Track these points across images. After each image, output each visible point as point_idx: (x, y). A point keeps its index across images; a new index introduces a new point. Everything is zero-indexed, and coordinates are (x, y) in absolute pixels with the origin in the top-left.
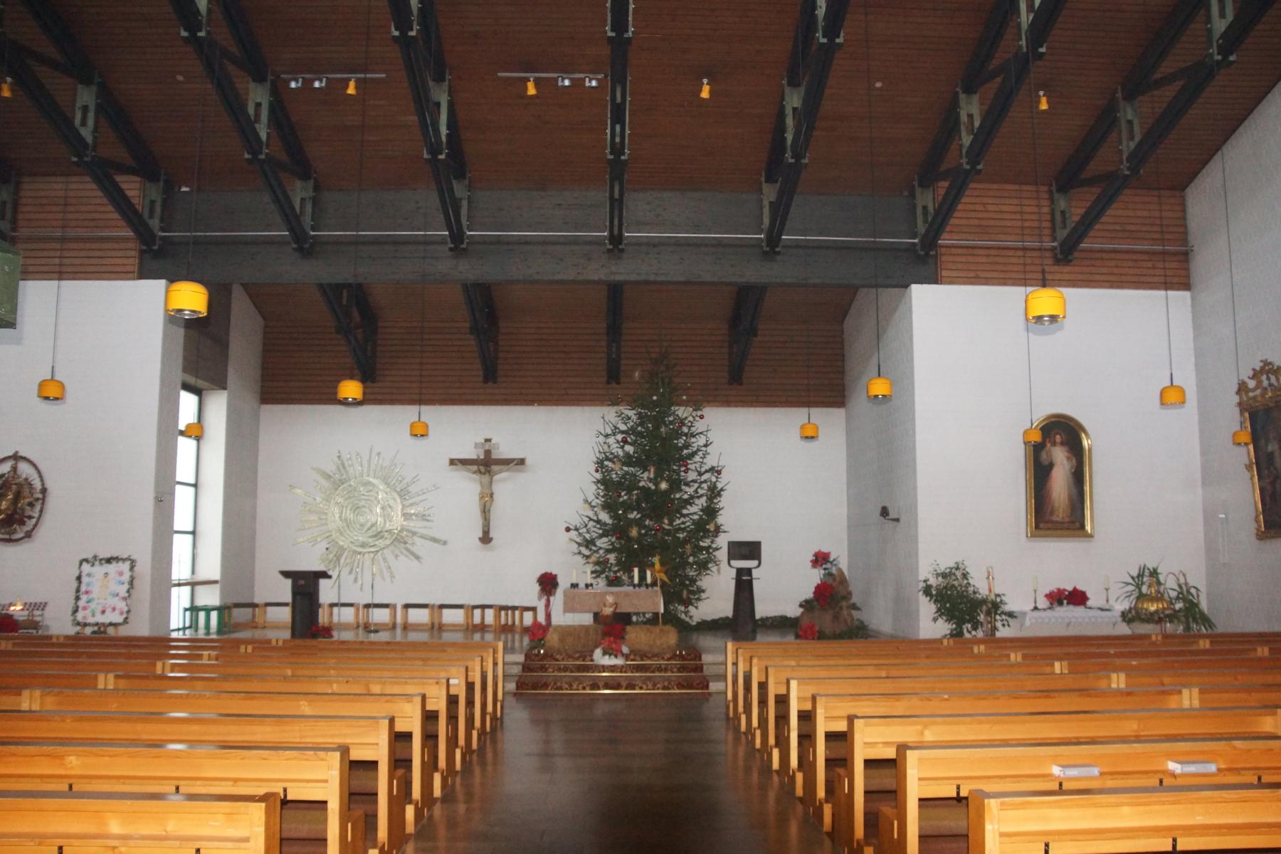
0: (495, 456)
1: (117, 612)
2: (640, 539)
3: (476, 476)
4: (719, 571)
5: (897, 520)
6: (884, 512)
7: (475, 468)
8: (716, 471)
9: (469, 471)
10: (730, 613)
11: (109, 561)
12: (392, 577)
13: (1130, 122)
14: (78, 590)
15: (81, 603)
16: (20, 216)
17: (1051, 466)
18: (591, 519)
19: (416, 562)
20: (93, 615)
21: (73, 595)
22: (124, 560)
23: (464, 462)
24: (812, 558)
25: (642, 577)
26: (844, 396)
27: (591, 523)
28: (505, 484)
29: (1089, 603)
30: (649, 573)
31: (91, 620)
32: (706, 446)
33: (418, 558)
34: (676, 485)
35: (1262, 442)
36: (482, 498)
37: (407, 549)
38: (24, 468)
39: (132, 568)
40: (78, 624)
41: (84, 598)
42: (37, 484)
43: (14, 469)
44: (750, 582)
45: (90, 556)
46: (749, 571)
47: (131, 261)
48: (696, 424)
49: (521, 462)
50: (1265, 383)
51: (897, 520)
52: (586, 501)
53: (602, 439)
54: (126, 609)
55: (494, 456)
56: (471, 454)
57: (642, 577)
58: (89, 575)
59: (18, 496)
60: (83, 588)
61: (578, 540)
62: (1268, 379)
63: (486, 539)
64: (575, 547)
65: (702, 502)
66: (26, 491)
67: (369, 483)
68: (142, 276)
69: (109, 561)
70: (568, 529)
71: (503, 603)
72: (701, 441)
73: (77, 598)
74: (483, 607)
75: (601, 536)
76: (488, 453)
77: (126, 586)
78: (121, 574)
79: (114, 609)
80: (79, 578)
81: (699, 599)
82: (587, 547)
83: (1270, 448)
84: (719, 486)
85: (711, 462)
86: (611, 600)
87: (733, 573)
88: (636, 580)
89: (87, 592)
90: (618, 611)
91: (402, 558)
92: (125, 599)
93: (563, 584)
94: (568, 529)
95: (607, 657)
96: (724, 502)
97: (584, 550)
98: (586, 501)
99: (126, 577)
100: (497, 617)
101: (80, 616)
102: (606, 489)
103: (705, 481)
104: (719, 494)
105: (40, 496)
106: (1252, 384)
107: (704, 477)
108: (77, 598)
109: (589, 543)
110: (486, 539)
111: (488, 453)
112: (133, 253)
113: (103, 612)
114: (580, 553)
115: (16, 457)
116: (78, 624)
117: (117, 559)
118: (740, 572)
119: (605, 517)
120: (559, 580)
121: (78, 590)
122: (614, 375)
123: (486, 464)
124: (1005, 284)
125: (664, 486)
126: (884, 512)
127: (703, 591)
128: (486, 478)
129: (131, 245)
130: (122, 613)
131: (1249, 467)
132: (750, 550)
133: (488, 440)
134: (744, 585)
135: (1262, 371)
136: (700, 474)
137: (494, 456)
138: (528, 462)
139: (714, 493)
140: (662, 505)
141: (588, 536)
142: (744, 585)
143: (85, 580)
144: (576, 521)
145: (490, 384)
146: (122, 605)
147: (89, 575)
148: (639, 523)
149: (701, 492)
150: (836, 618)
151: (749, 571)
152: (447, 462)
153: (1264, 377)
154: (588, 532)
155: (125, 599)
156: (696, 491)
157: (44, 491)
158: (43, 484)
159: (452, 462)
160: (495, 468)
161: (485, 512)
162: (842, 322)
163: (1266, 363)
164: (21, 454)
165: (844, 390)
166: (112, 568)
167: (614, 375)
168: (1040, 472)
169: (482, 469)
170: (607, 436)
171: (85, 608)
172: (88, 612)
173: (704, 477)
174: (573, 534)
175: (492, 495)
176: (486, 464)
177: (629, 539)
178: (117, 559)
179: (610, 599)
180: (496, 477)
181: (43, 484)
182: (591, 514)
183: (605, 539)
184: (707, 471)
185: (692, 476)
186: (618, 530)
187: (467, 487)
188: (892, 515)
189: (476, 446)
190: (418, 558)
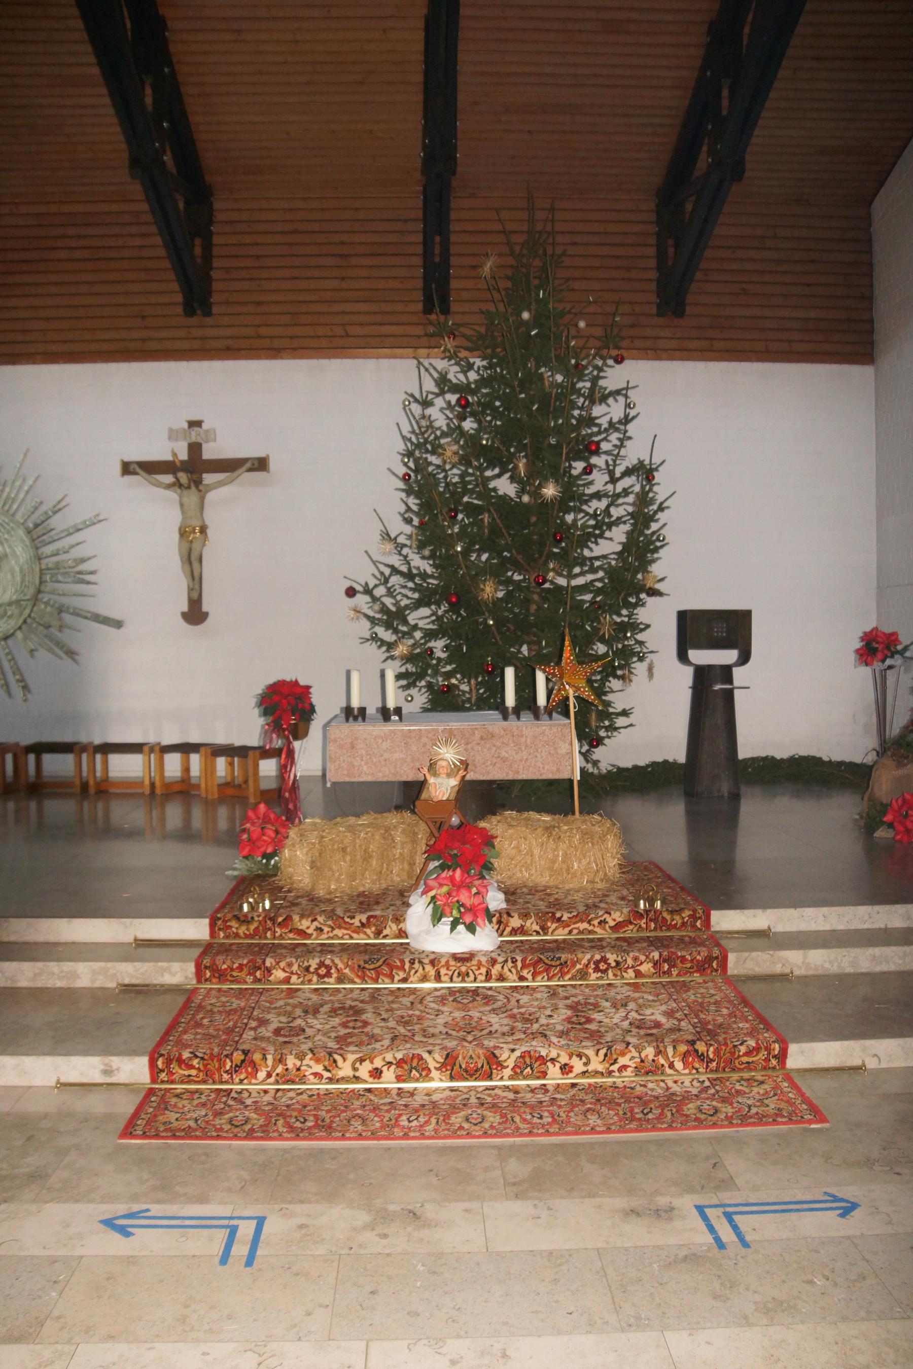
0: (209, 452)
2: (496, 606)
3: (172, 495)
4: (650, 669)
7: (169, 479)
8: (645, 472)
9: (159, 485)
10: (679, 754)
12: (25, 688)
18: (395, 570)
19: (67, 661)
23: (150, 468)
24: (858, 645)
25: (526, 686)
26: (872, 343)
27: (395, 580)
28: (228, 505)
30: (540, 678)
32: (626, 420)
34: (572, 496)
44: (729, 696)
46: (726, 673)
48: (608, 372)
49: (261, 464)
52: (386, 536)
53: (416, 409)
55: (206, 456)
56: (160, 450)
57: (526, 686)
63: (195, 614)
65: (619, 534)
71: (221, 739)
72: (615, 410)
74: (186, 749)
75: (418, 604)
76: (195, 448)
81: (612, 728)
82: (388, 625)
85: (633, 454)
86: (448, 753)
87: (687, 674)
88: (510, 700)
90: (468, 778)
91: (42, 654)
93: (326, 704)
94: (351, 592)
96: (671, 524)
97: (381, 632)
98: (386, 536)
100: (208, 769)
102: (426, 507)
103: (626, 492)
104: (651, 518)
107: (620, 487)
109: (393, 618)
110: (195, 614)
111: (195, 448)
114: (374, 638)
118: (703, 675)
119: (420, 563)
120: (316, 698)
122: (436, 295)
123: (191, 469)
125: (550, 491)
127: (625, 713)
128: (192, 497)
132: (729, 629)
133: (195, 424)
134: (712, 701)
136: (613, 480)
137: (206, 456)
138: (272, 465)
139: (644, 514)
140: (538, 534)
141: (388, 601)
142: (712, 701)
144: (365, 574)
145: (194, 320)
148: (497, 572)
149: (615, 512)
151: (726, 673)
152: (118, 469)
154: (390, 593)
156: (607, 511)
159: (127, 468)
160: (209, 478)
161: (192, 561)
162: (871, 202)
165: (871, 332)
167: (436, 295)
169: (183, 477)
170: (426, 404)
173: (620, 487)
174: (362, 600)
175: (203, 530)
176: (191, 469)
177: (476, 607)
179: (448, 755)
180: (211, 496)
182: (395, 560)
183: (425, 611)
184: (628, 473)
185: (599, 480)
186: (451, 590)
187: (156, 512)
189: (173, 435)
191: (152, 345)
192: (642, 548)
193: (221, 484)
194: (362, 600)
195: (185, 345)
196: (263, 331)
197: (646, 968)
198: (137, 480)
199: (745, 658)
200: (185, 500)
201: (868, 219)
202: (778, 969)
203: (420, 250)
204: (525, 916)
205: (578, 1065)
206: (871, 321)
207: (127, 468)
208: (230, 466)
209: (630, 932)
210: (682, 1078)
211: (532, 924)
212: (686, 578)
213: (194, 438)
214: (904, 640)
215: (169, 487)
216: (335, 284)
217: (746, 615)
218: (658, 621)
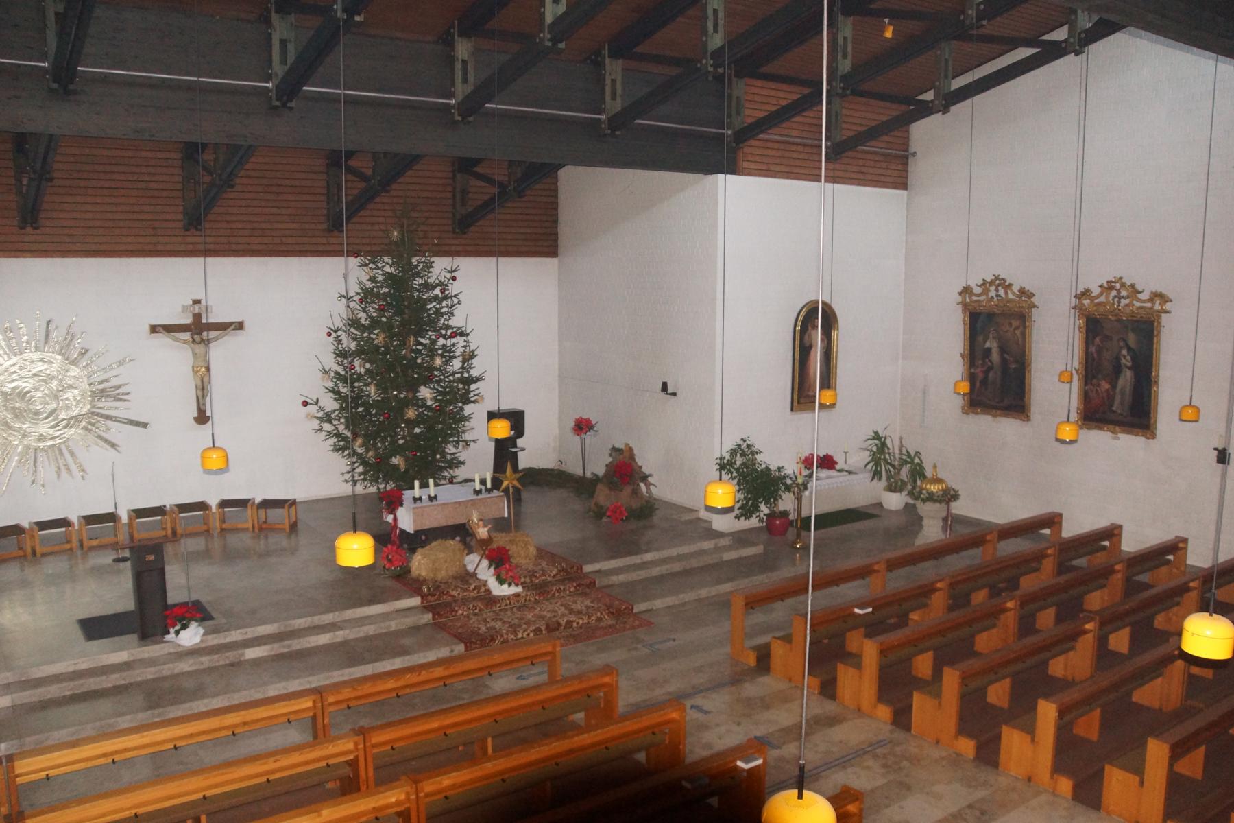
5: (674, 394)
6: (664, 387)
7: (186, 336)
9: (177, 340)
13: (946, 60)
17: (811, 347)
23: (169, 329)
24: (573, 424)
28: (222, 351)
29: (838, 467)
33: (113, 446)
35: (980, 338)
36: (195, 372)
37: (100, 437)
49: (240, 326)
50: (992, 293)
51: (674, 394)
61: (321, 414)
62: (997, 290)
64: (316, 424)
70: (305, 404)
76: (197, 316)
83: (988, 345)
85: (456, 322)
106: (977, 290)
110: (202, 418)
123: (199, 329)
124: (788, 178)
126: (664, 387)
128: (200, 349)
131: (962, 356)
133: (197, 302)
135: (991, 283)
138: (246, 325)
142: (505, 452)
152: (148, 328)
153: (993, 288)
159: (154, 329)
163: (997, 278)
168: (802, 352)
169: (197, 338)
175: (208, 369)
176: (199, 329)
187: (175, 358)
189: (184, 308)
190: (113, 446)
191: (160, 247)
193: (216, 339)
194: (312, 409)
195: (182, 248)
200: (197, 351)
208: (223, 327)
213: (197, 311)
215: (185, 342)
216: (275, 210)
218: (476, 413)
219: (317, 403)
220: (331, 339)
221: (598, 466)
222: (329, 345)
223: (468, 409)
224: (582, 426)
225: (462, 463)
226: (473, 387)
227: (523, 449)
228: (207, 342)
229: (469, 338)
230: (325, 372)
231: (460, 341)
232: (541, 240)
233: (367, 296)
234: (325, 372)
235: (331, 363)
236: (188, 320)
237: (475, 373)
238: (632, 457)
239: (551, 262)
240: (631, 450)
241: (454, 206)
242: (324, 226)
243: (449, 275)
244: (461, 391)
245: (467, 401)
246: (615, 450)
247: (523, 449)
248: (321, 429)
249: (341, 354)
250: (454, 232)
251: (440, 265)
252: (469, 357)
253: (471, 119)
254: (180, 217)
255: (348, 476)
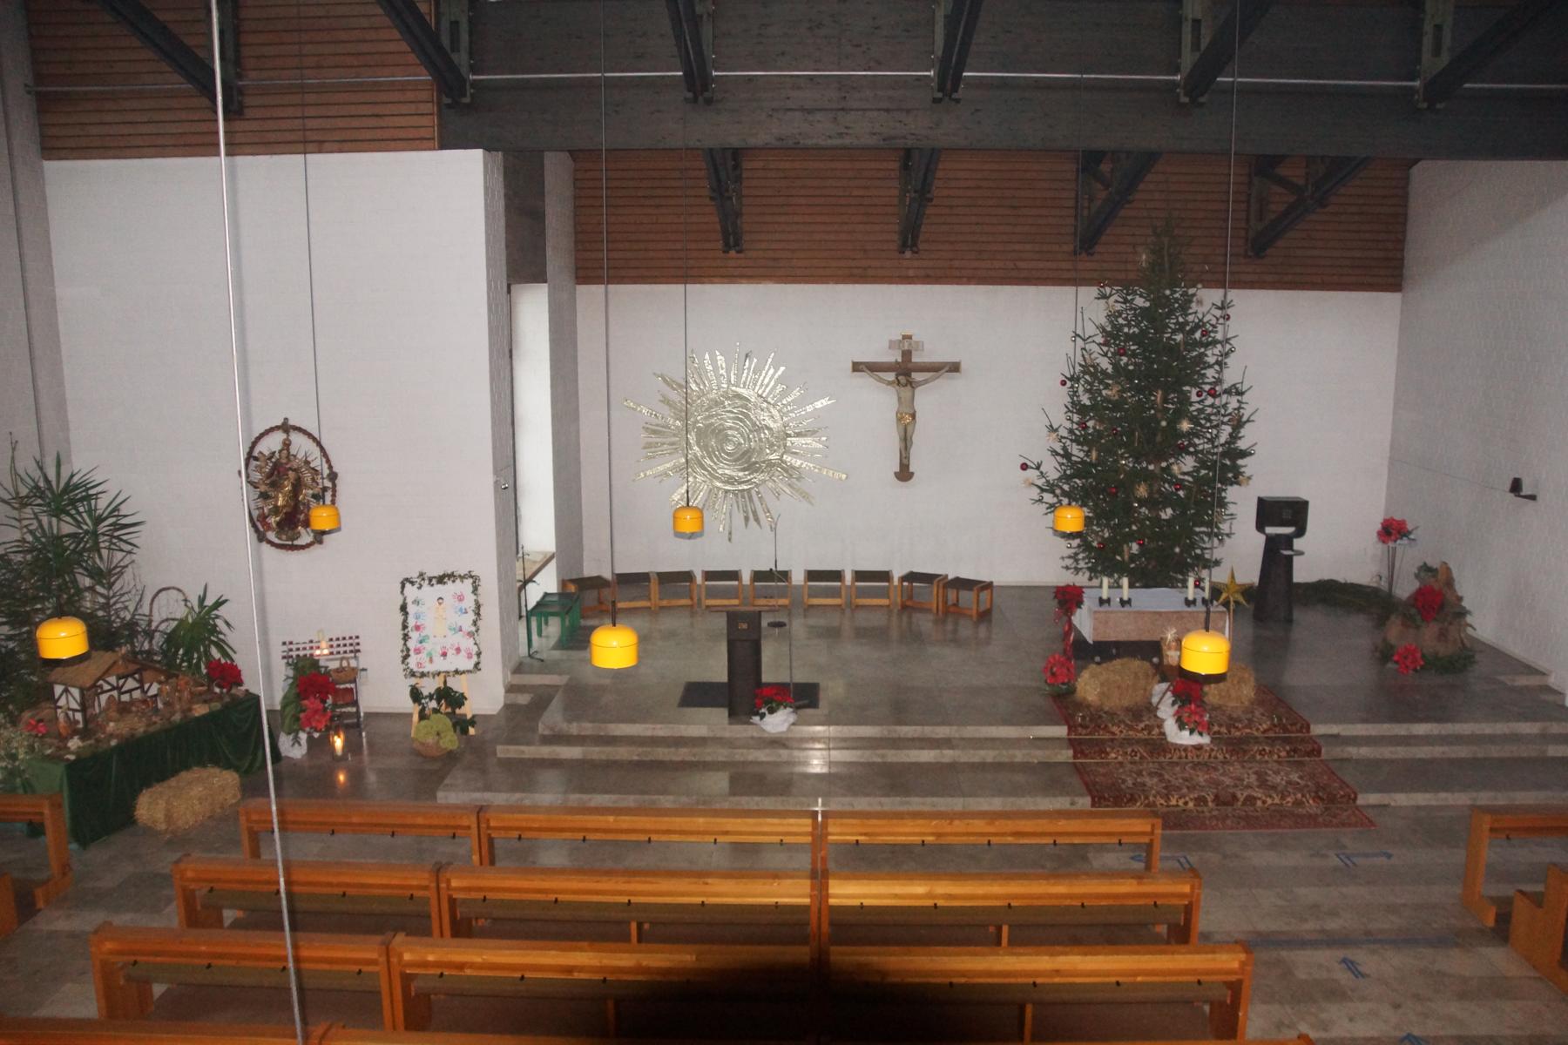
1: (463, 653)
5: (1533, 498)
6: (1516, 486)
7: (891, 376)
9: (881, 380)
11: (441, 580)
14: (405, 627)
15: (412, 644)
16: (246, 51)
20: (431, 660)
21: (400, 634)
22: (462, 578)
23: (873, 368)
24: (1379, 527)
26: (1401, 276)
28: (929, 398)
31: (428, 668)
36: (899, 420)
38: (301, 446)
39: (475, 590)
40: (413, 674)
41: (414, 635)
42: (317, 462)
43: (287, 445)
45: (414, 575)
47: (425, 121)
49: (955, 368)
51: (1533, 498)
54: (475, 649)
55: (915, 359)
58: (417, 602)
59: (298, 485)
60: (411, 622)
61: (1041, 482)
63: (904, 474)
64: (1035, 493)
66: (307, 477)
67: (739, 396)
68: (444, 145)
69: (441, 580)
70: (1024, 467)
73: (406, 637)
76: (907, 354)
77: (472, 617)
78: (461, 598)
79: (458, 650)
80: (404, 608)
84: (1246, 413)
85: (1230, 377)
87: (1261, 539)
89: (417, 628)
92: (470, 634)
94: (1024, 467)
95: (1186, 733)
99: (469, 602)
101: (413, 662)
105: (328, 484)
108: (406, 637)
110: (904, 474)
111: (907, 354)
112: (428, 108)
113: (444, 655)
115: (286, 427)
116: (413, 674)
117: (452, 576)
121: (405, 627)
123: (905, 371)
126: (1516, 486)
128: (906, 392)
129: (424, 95)
130: (470, 656)
133: (907, 337)
138: (963, 366)
142: (1277, 557)
143: (411, 609)
146: (467, 644)
147: (417, 602)
150: (1442, 635)
155: (470, 634)
157: (333, 476)
158: (330, 467)
159: (857, 367)
161: (906, 441)
164: (291, 423)
165: (1401, 267)
166: (450, 588)
171: (418, 651)
172: (423, 656)
175: (913, 416)
176: (905, 371)
178: (452, 576)
180: (917, 391)
181: (330, 467)
184: (1228, 392)
187: (880, 399)
188: (1526, 491)
189: (892, 344)
192: (1235, 454)
193: (926, 381)
194: (1032, 474)
196: (956, 263)
197: (1283, 754)
198: (865, 379)
199: (1301, 532)
201: (1407, 179)
202: (1345, 756)
203: (1071, 203)
204: (1220, 725)
205: (1269, 801)
206: (1402, 259)
207: (857, 367)
208: (935, 369)
209: (1271, 734)
210: (1312, 806)
211: (1224, 730)
212: (1268, 475)
214: (1410, 527)
215: (890, 383)
217: (1305, 504)
218: (1241, 503)
219: (1038, 468)
220: (1065, 389)
221: (1405, 588)
222: (1062, 396)
223: (1232, 493)
224: (1392, 531)
225: (1217, 563)
226: (1240, 462)
227: (1301, 553)
228: (912, 384)
229: (1245, 398)
230: (1052, 429)
231: (1233, 403)
232: (1377, 262)
233: (1112, 335)
234: (1052, 429)
235: (1060, 418)
236: (894, 357)
237: (1242, 445)
238: (1450, 582)
239: (1391, 300)
240: (1448, 569)
241: (1248, 220)
242: (1070, 248)
243: (1218, 313)
244: (1227, 465)
245: (1236, 481)
246: (1426, 568)
247: (1301, 553)
248: (1040, 501)
249: (1077, 407)
250: (1246, 256)
251: (1206, 300)
252: (1238, 424)
253: (1202, 100)
254: (896, 237)
255: (1069, 562)
